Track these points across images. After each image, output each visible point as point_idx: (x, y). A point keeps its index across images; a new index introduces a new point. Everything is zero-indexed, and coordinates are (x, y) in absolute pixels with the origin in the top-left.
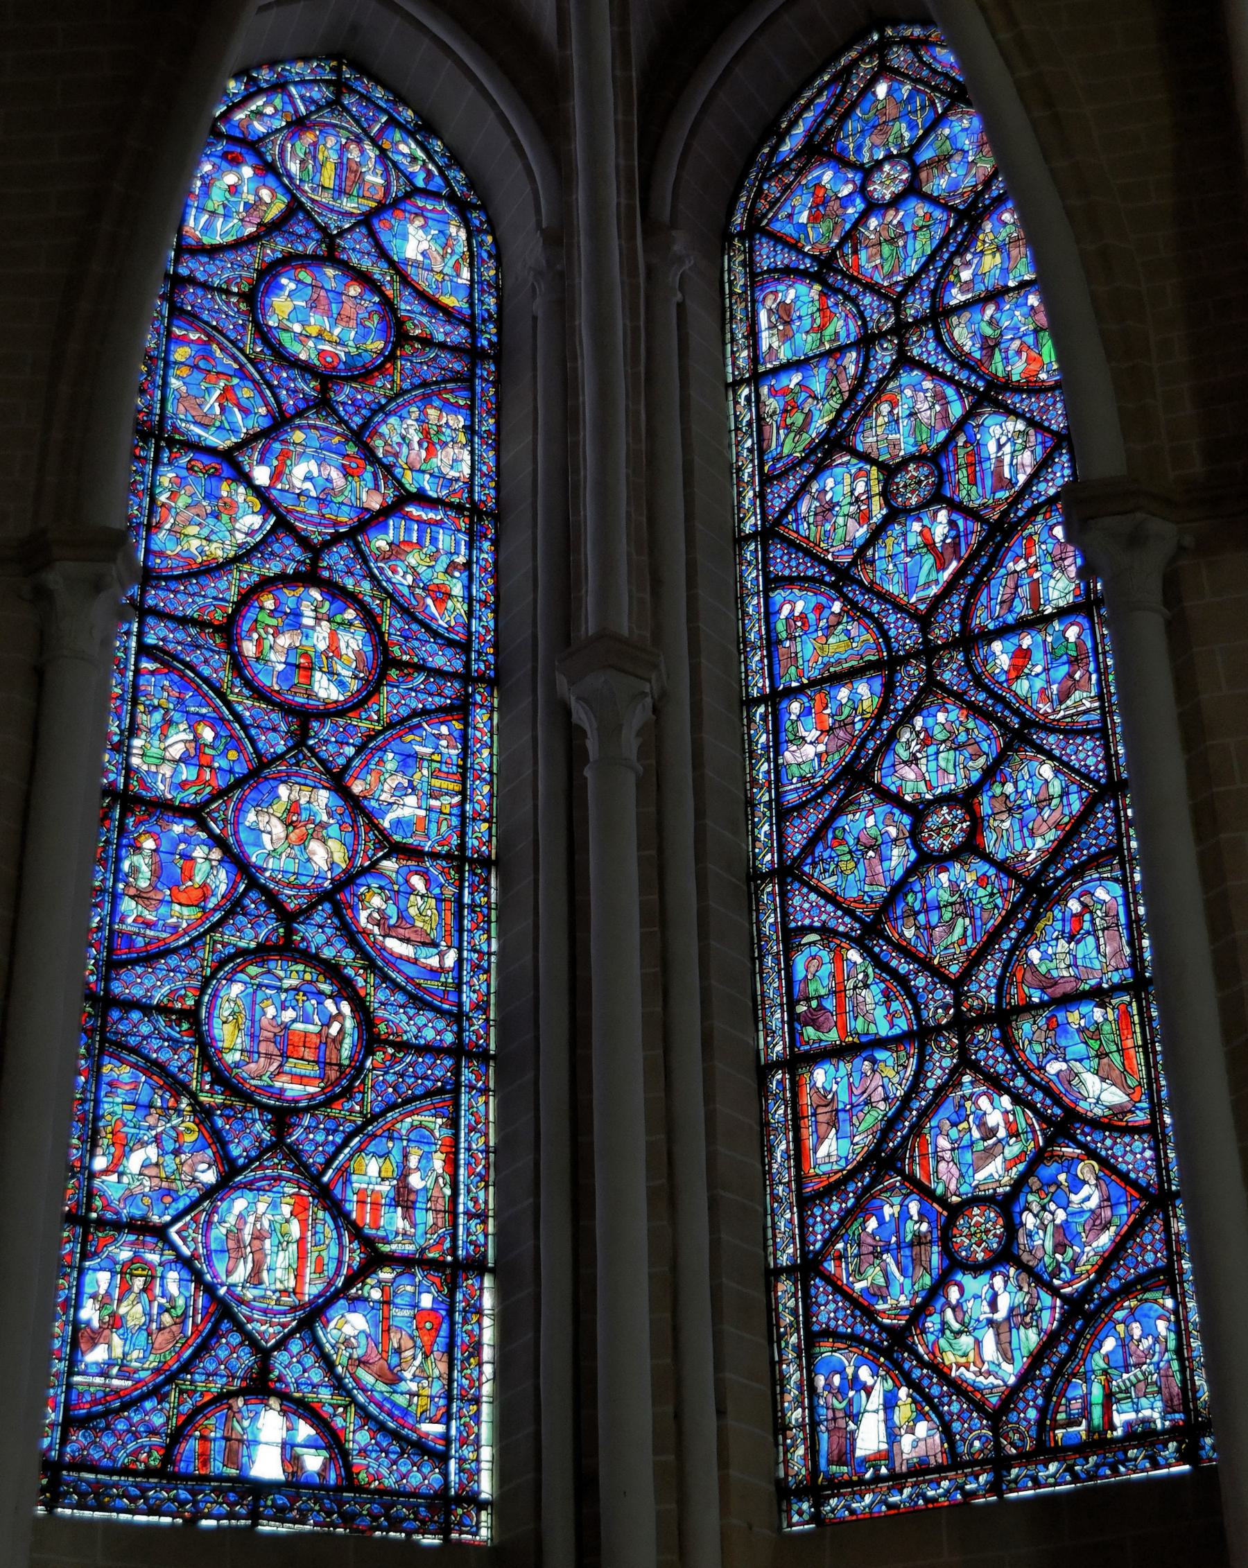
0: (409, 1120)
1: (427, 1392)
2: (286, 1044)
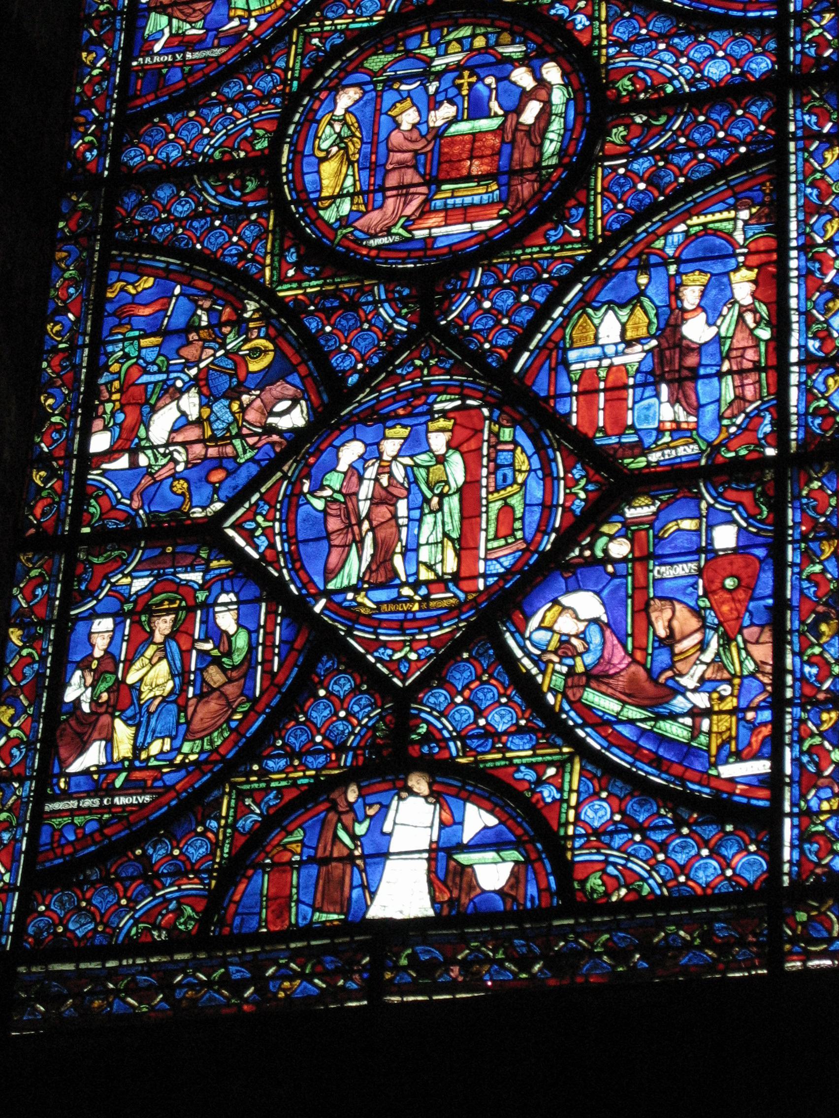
0: (682, 227)
1: (729, 705)
2: (438, 161)
